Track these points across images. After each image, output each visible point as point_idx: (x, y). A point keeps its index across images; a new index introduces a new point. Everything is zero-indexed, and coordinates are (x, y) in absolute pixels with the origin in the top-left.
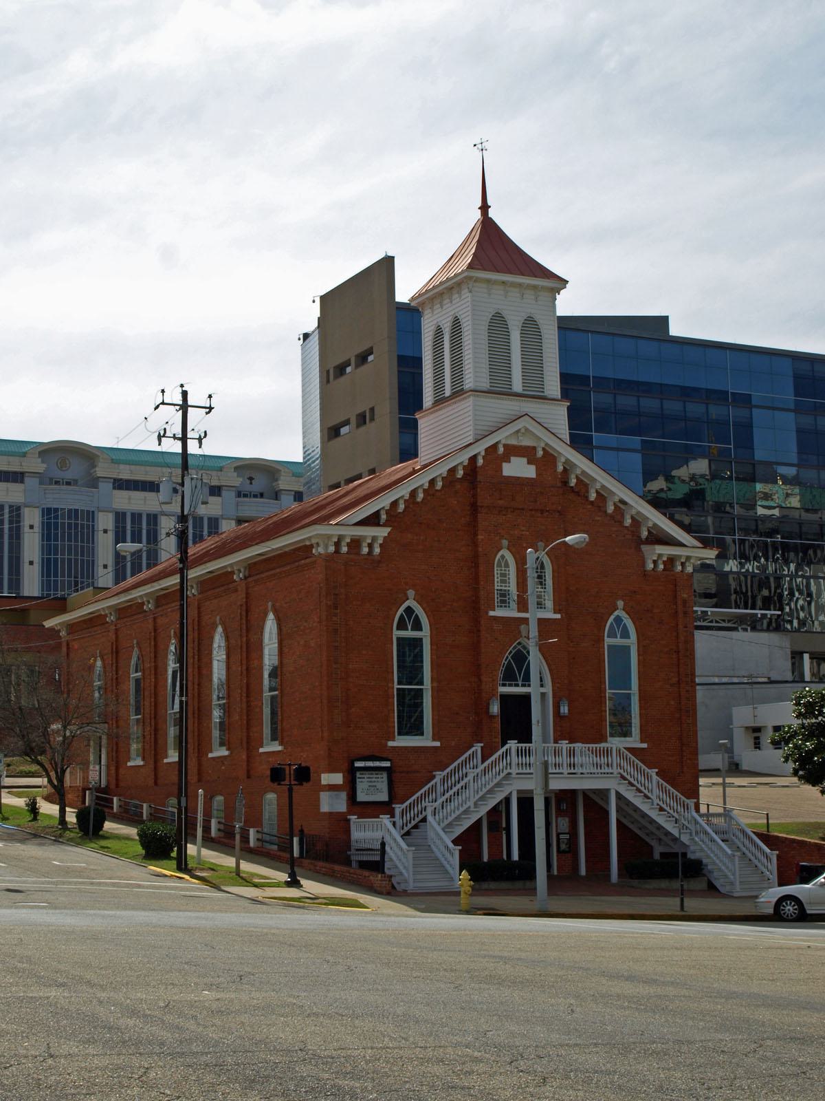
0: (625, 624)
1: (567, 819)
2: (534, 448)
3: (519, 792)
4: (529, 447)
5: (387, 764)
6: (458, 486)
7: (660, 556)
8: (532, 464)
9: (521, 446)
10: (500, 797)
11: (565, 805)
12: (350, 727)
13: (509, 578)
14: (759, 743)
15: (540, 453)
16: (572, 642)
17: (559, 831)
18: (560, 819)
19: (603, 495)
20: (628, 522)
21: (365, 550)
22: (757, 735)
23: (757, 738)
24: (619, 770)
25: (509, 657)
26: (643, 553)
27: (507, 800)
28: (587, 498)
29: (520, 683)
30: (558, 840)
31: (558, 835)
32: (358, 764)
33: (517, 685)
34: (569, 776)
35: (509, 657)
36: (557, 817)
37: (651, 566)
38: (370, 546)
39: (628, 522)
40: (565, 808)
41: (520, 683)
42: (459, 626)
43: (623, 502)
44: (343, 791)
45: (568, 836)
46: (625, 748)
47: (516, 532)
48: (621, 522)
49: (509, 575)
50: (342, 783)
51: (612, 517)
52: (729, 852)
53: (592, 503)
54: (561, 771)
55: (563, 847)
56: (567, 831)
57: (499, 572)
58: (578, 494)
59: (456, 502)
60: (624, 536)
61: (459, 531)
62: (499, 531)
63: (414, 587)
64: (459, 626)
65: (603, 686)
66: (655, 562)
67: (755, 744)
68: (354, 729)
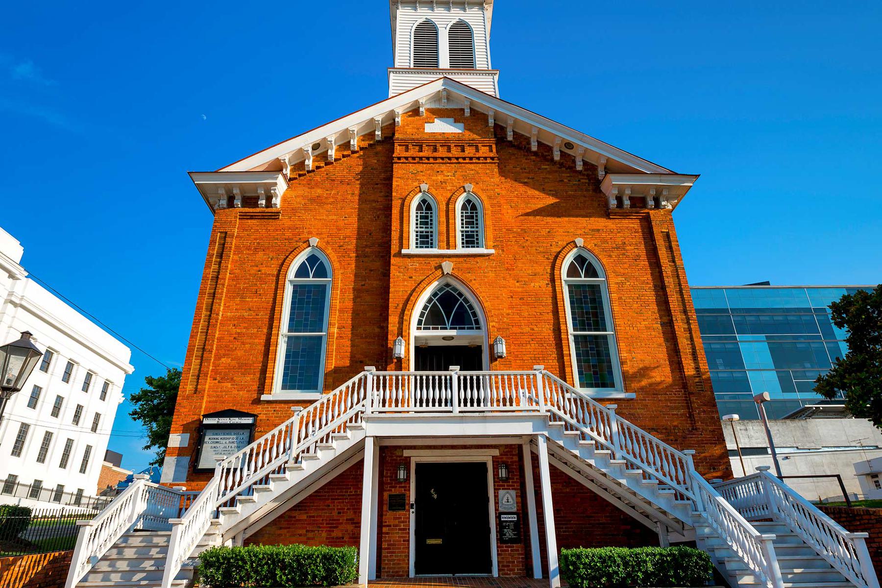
0: (590, 264)
1: (513, 493)
2: (463, 110)
3: (377, 439)
4: (455, 109)
5: (249, 421)
6: (379, 148)
7: (621, 188)
8: (460, 122)
9: (447, 109)
10: (339, 447)
11: (504, 470)
12: (216, 380)
13: (431, 220)
14: (879, 485)
15: (467, 113)
16: (517, 282)
17: (501, 510)
18: (501, 492)
19: (548, 146)
20: (579, 167)
21: (263, 202)
22: (876, 479)
23: (876, 482)
24: (549, 407)
25: (435, 300)
26: (604, 195)
27: (360, 447)
28: (529, 149)
29: (448, 328)
30: (501, 525)
31: (498, 517)
32: (206, 421)
33: (446, 329)
34: (461, 415)
35: (435, 300)
36: (496, 490)
37: (613, 203)
38: (269, 198)
39: (579, 167)
40: (504, 475)
41: (448, 326)
42: (371, 271)
43: (569, 145)
44: (187, 455)
45: (514, 518)
46: (595, 399)
47: (439, 178)
48: (572, 168)
49: (431, 217)
50: (187, 446)
51: (561, 165)
52: (755, 533)
53: (535, 154)
54: (449, 408)
55: (509, 534)
56: (515, 510)
57: (419, 215)
58: (518, 148)
59: (376, 161)
60: (579, 181)
61: (377, 184)
62: (418, 178)
63: (319, 234)
64: (371, 271)
65: (563, 327)
66: (619, 199)
67: (876, 486)
68: (219, 382)
